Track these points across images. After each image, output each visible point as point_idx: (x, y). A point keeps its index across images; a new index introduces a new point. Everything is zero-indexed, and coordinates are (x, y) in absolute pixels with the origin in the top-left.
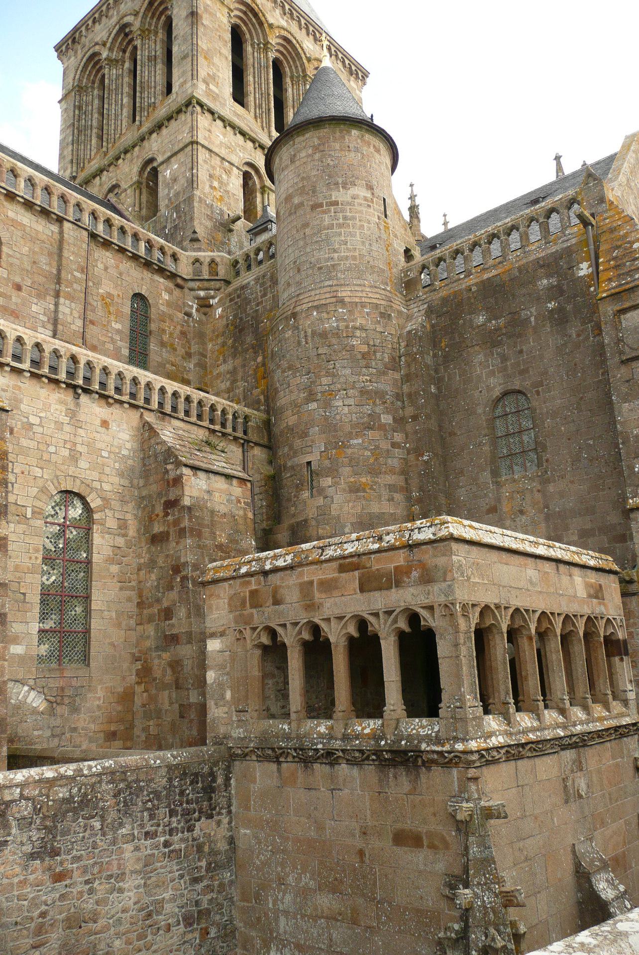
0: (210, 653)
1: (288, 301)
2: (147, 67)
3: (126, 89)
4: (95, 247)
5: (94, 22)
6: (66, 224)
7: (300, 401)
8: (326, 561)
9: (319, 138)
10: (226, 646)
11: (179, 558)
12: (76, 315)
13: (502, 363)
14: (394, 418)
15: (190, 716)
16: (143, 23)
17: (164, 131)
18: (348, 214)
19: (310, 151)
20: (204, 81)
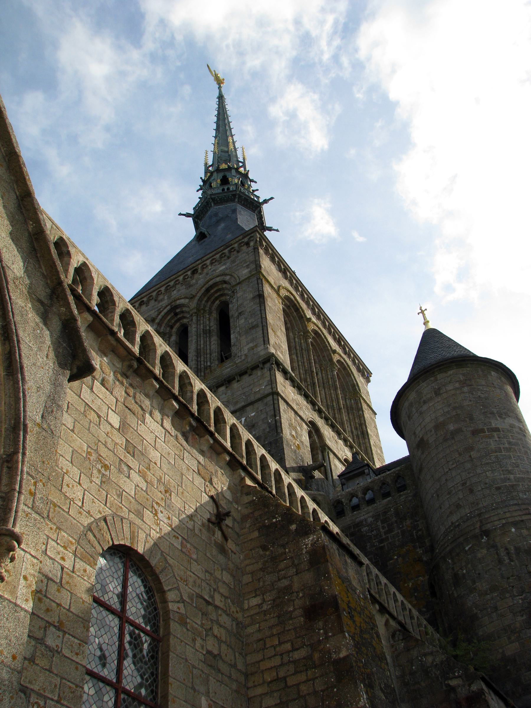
2: (202, 338)
7: (518, 625)
9: (463, 375)
18: (511, 440)
19: (457, 385)
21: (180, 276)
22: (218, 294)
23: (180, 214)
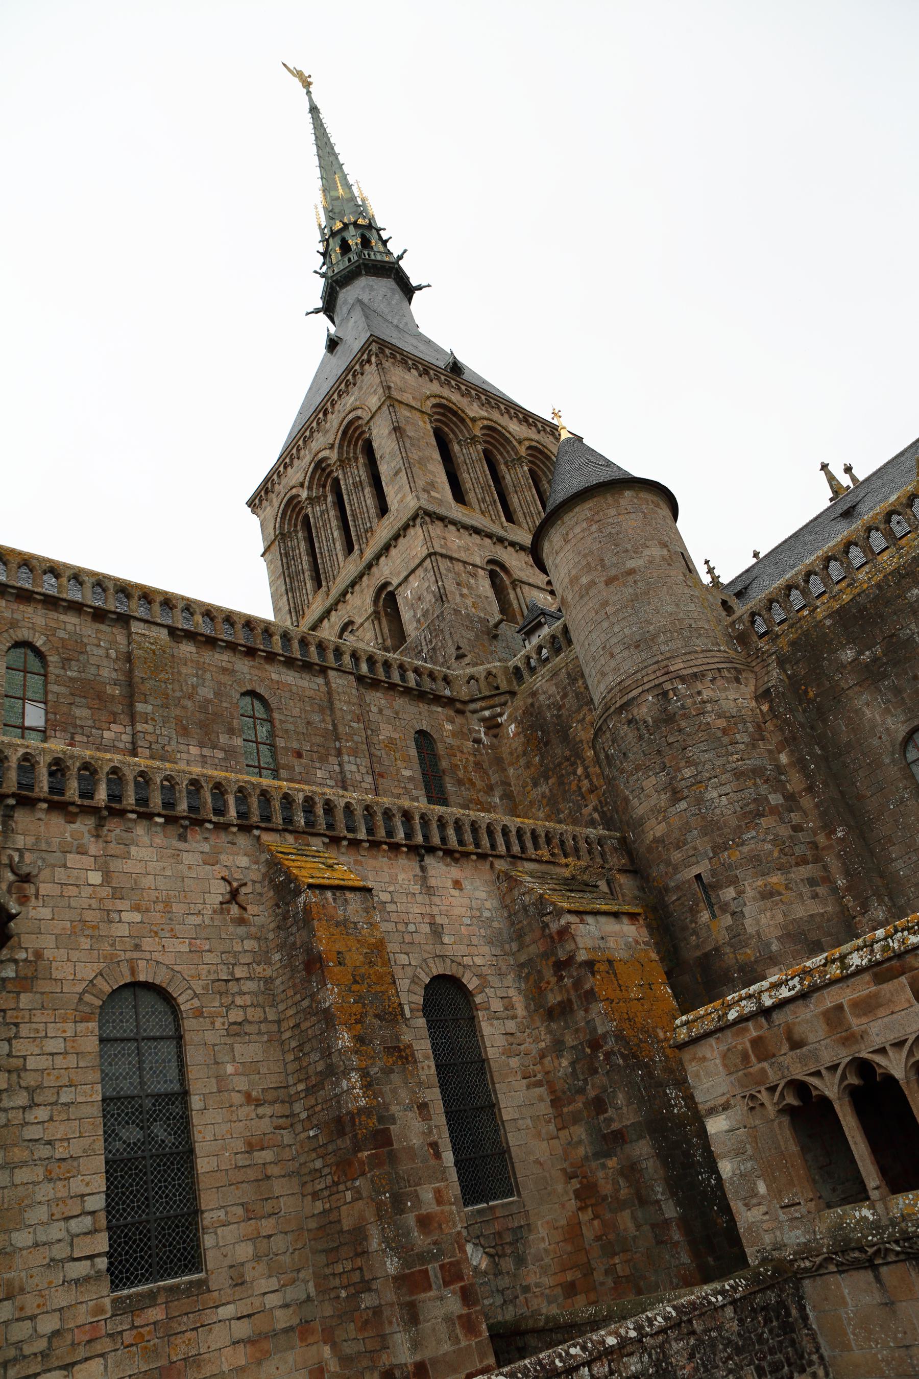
0: (714, 1137)
1: (608, 693)
3: (334, 523)
4: (364, 691)
5: (285, 467)
6: (331, 674)
7: (663, 804)
8: (853, 974)
9: (590, 509)
10: (737, 1121)
11: (595, 1029)
12: (364, 771)
13: (895, 696)
14: (784, 796)
15: (671, 1238)
16: (340, 453)
17: (393, 552)
19: (585, 525)
20: (424, 490)
21: (312, 422)
22: (358, 432)
23: (308, 314)
